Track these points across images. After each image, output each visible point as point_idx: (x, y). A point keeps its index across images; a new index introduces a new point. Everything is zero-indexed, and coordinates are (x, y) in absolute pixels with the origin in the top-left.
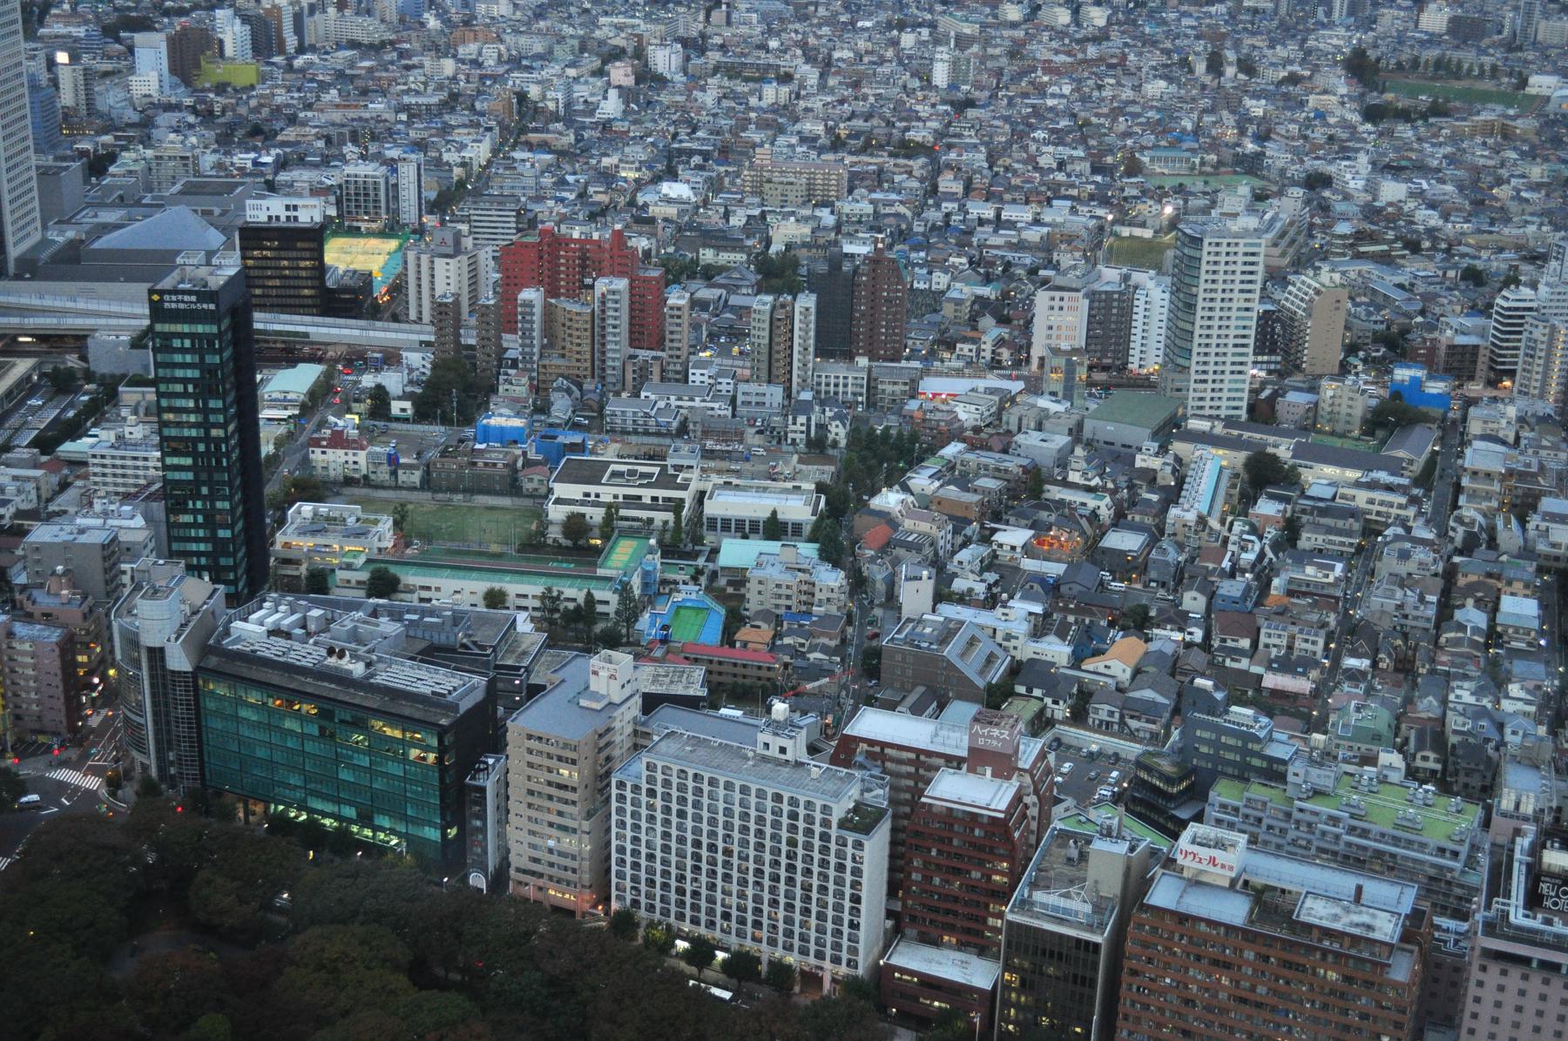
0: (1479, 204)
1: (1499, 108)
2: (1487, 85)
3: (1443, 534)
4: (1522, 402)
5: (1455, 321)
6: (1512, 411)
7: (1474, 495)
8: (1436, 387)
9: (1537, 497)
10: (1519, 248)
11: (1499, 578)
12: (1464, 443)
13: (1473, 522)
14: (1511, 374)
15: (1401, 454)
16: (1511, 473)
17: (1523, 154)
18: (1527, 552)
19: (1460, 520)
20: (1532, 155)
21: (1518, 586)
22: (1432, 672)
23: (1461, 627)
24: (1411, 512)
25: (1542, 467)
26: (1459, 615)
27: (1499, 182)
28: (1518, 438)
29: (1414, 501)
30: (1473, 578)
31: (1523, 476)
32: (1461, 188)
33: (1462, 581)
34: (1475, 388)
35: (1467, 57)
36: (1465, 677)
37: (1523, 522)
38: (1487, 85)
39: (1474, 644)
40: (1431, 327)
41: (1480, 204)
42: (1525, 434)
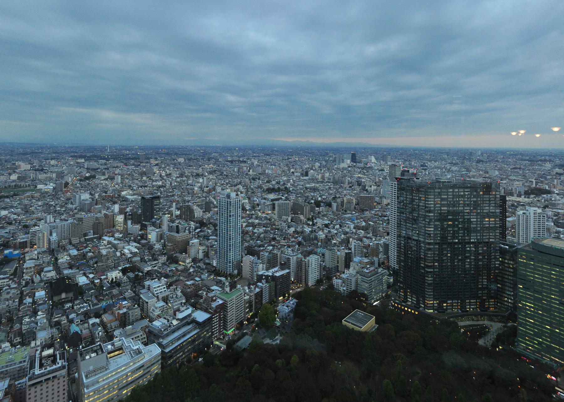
0: (27, 212)
1: (31, 192)
2: (28, 188)
3: (19, 283)
4: (38, 250)
5: (20, 237)
6: (36, 252)
7: (27, 273)
8: (16, 252)
9: (43, 269)
10: (37, 219)
11: (34, 289)
12: (24, 262)
13: (27, 279)
14: (36, 244)
15: (7, 269)
16: (36, 265)
17: (37, 200)
18: (42, 281)
19: (24, 280)
20: (39, 200)
21: (39, 289)
22: (18, 318)
23: (25, 304)
24: (10, 282)
25: (43, 262)
26: (24, 301)
27: (31, 207)
28: (38, 257)
29: (10, 279)
30: (27, 292)
31: (39, 265)
32: (22, 210)
33: (25, 293)
34: (27, 250)
35: (23, 184)
36: (27, 315)
37: (40, 275)
38: (28, 188)
39: (28, 307)
40: (15, 240)
41: (26, 210)
42: (40, 256)
